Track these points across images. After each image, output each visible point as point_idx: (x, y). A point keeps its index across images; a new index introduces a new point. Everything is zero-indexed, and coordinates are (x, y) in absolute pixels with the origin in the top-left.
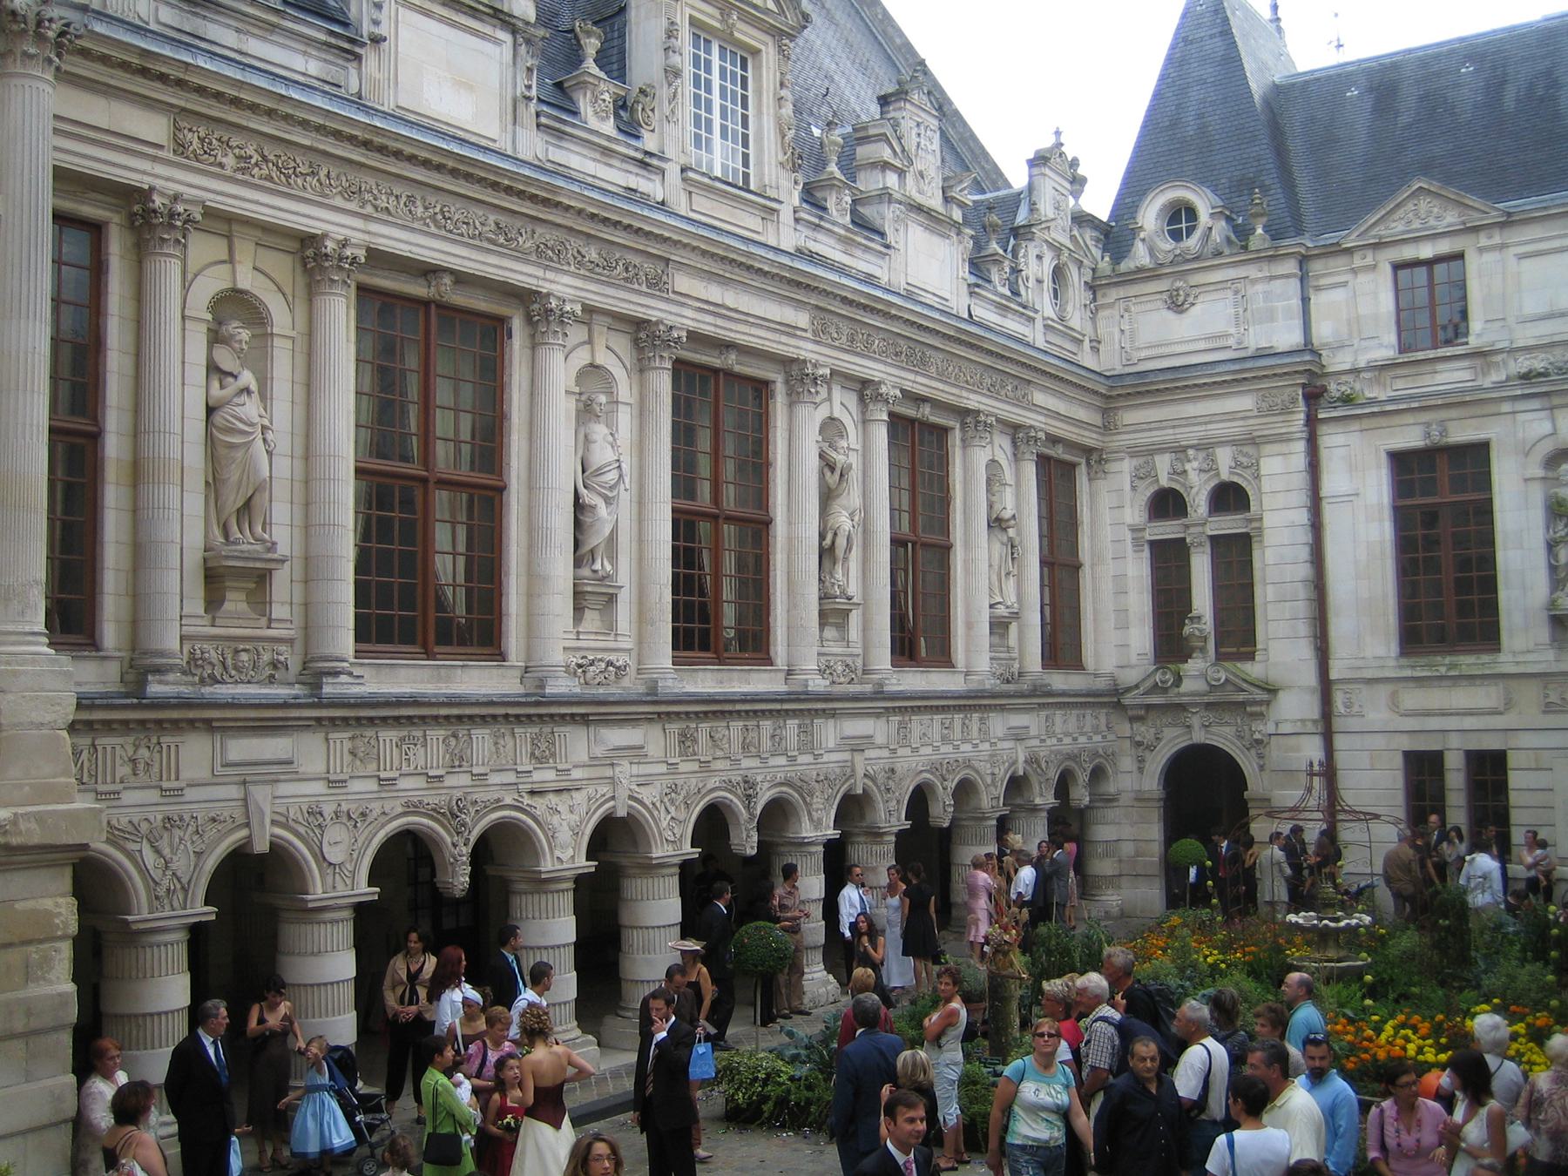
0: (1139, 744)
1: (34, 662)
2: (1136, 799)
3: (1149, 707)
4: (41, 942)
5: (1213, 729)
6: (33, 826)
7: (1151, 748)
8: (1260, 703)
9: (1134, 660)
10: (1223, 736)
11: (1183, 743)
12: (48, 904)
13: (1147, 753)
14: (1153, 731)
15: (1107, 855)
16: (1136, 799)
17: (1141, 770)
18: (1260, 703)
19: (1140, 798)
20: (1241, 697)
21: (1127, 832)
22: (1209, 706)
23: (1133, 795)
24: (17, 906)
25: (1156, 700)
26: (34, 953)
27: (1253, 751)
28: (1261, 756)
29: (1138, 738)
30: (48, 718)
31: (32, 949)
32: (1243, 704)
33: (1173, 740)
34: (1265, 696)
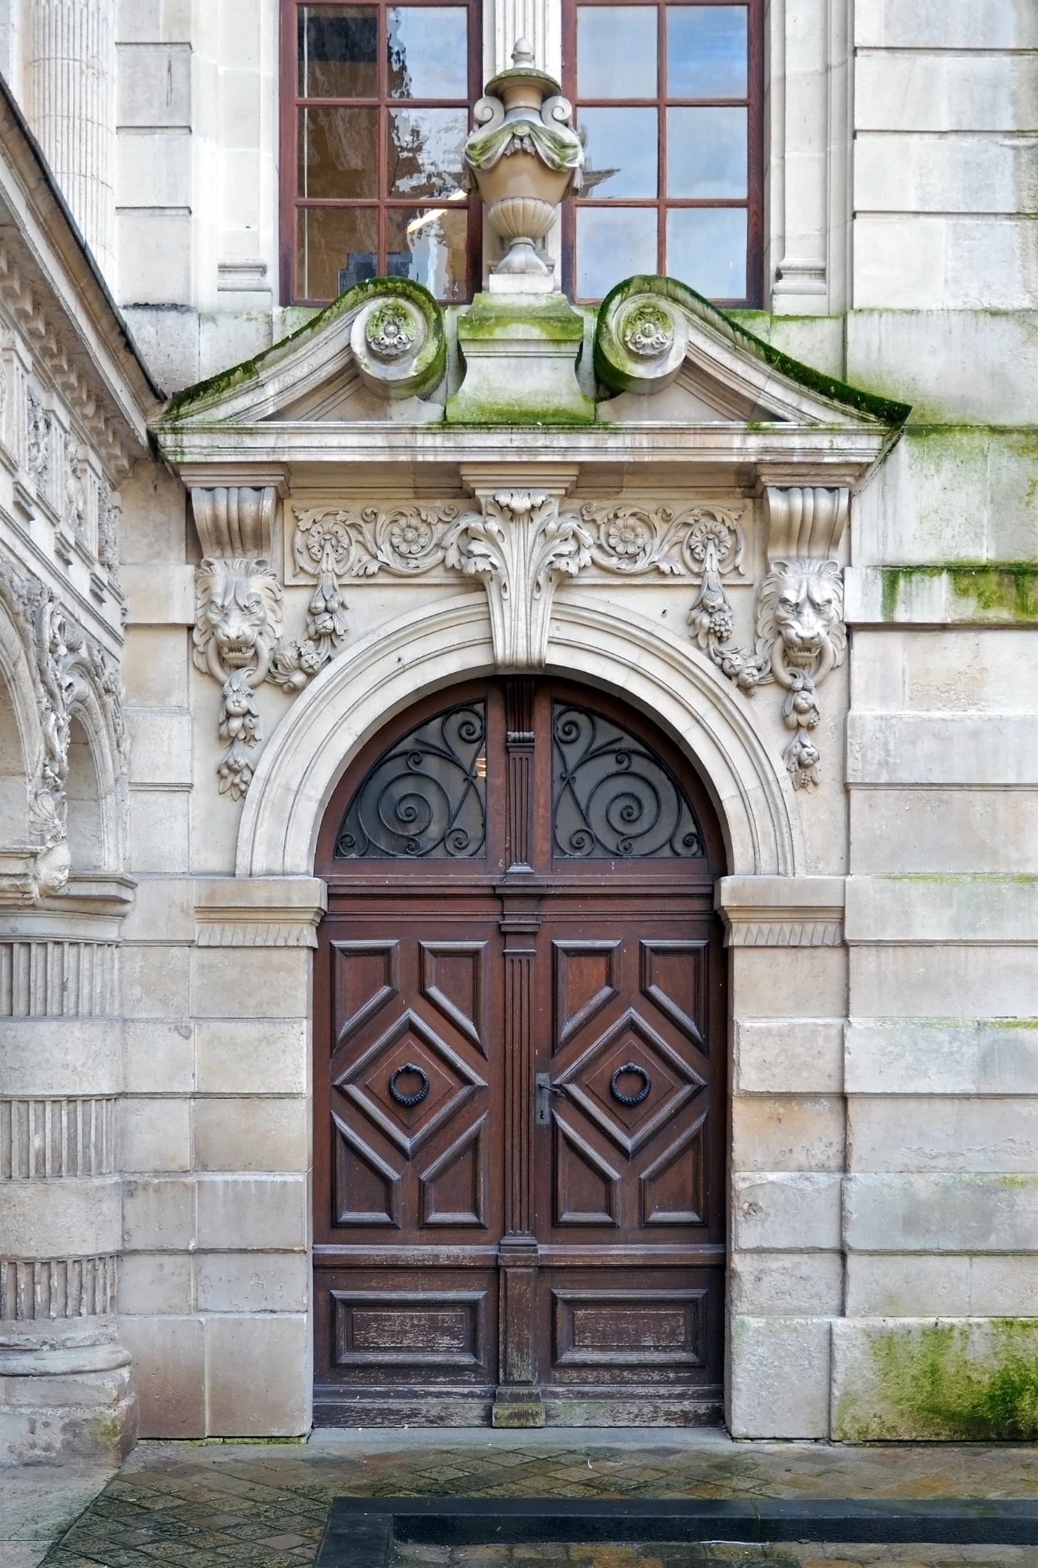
0: (232, 655)
2: (210, 912)
3: (291, 480)
5: (576, 598)
7: (285, 681)
8: (812, 473)
9: (205, 290)
10: (629, 632)
11: (448, 656)
13: (266, 703)
14: (296, 601)
15: (67, 1163)
16: (210, 912)
17: (233, 779)
18: (812, 473)
19: (227, 907)
20: (742, 446)
21: (161, 1057)
22: (591, 481)
23: (193, 894)
25: (340, 441)
27: (768, 699)
28: (796, 722)
29: (235, 627)
32: (748, 482)
33: (397, 644)
34: (863, 444)
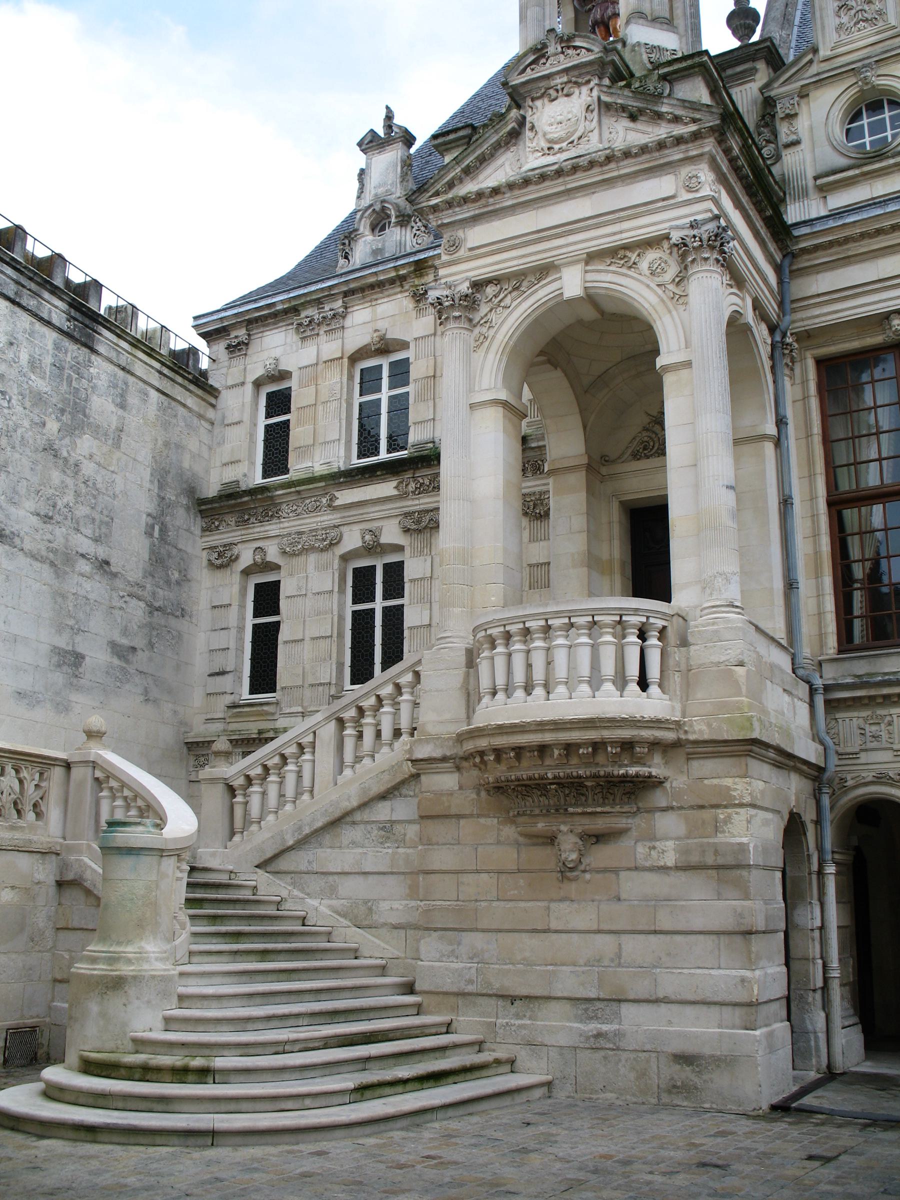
1: (713, 624)
4: (726, 807)
6: (704, 727)
12: (728, 782)
24: (706, 782)
26: (721, 814)
30: (723, 658)
31: (719, 811)
